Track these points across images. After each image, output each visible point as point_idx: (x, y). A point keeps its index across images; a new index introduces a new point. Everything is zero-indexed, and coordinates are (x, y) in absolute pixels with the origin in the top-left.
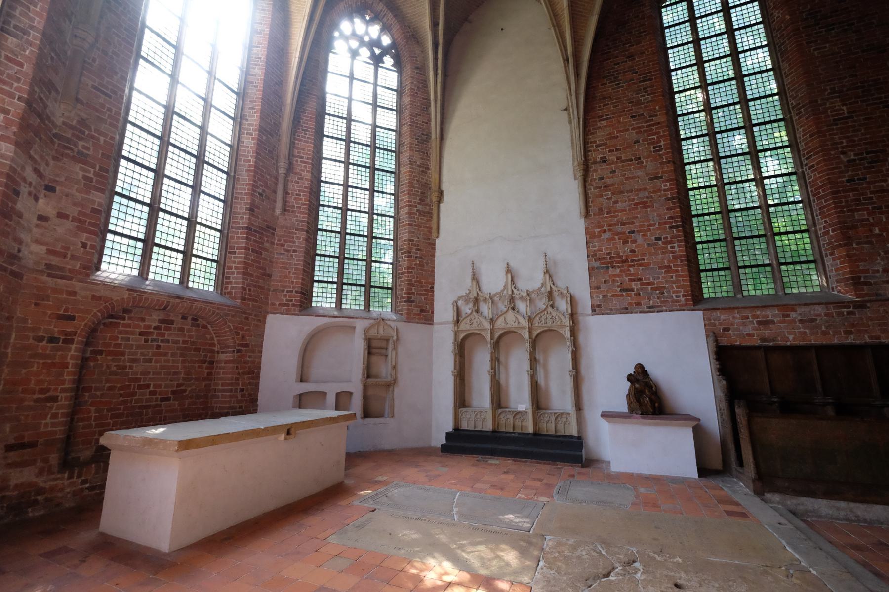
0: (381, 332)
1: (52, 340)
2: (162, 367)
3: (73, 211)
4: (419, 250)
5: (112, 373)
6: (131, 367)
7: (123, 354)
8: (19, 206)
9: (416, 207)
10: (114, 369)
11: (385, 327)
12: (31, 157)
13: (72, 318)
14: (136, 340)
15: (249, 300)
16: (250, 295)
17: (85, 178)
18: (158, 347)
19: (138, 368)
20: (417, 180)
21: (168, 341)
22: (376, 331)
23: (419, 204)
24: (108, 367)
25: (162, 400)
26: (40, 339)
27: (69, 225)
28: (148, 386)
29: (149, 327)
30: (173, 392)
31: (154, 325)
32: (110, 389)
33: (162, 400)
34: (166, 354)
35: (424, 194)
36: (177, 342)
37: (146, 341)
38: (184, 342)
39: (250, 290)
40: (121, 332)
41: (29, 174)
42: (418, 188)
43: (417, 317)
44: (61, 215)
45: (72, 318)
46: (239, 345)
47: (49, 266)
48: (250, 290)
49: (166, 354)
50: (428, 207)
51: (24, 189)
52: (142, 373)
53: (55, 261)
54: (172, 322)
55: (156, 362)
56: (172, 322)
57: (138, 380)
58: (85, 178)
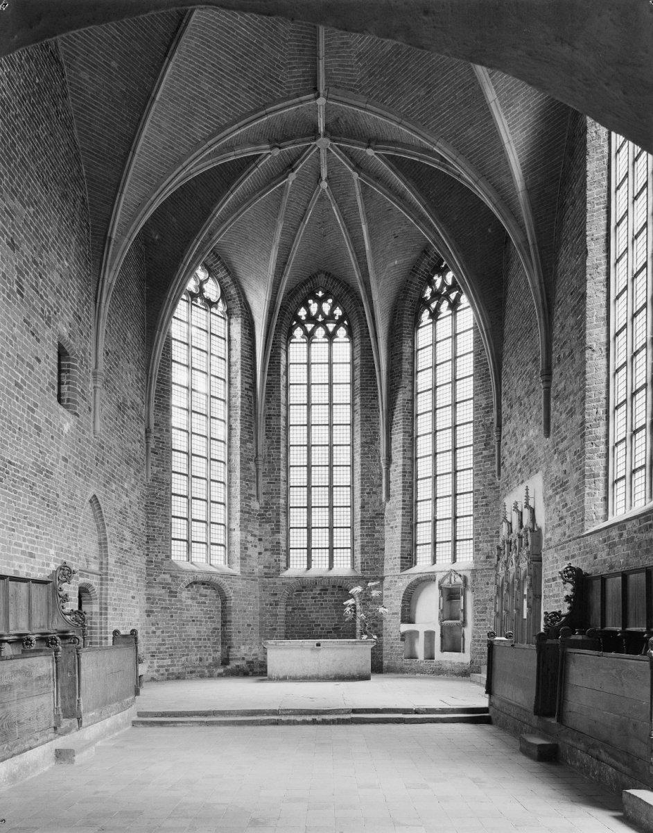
1: (271, 605)
2: (325, 615)
3: (269, 546)
4: (485, 497)
5: (302, 618)
6: (310, 616)
7: (305, 609)
8: (248, 553)
9: (482, 453)
10: (302, 616)
12: (249, 531)
13: (276, 594)
14: (311, 601)
15: (368, 570)
16: (367, 566)
17: (272, 529)
18: (322, 604)
19: (314, 616)
20: (483, 425)
21: (326, 601)
23: (484, 449)
24: (300, 616)
25: (328, 632)
26: (267, 605)
27: (269, 553)
28: (319, 625)
29: (315, 594)
30: (333, 629)
31: (318, 592)
32: (302, 626)
33: (328, 632)
34: (326, 608)
35: (490, 436)
36: (331, 601)
37: (315, 602)
38: (336, 601)
39: (367, 563)
40: (303, 598)
41: (250, 538)
42: (483, 433)
44: (266, 550)
45: (276, 594)
46: (364, 600)
47: (265, 574)
48: (367, 563)
49: (326, 608)
50: (492, 450)
51: (249, 546)
52: (316, 619)
53: (266, 570)
54: (327, 590)
55: (321, 612)
56: (327, 590)
57: (314, 622)
58: (272, 529)
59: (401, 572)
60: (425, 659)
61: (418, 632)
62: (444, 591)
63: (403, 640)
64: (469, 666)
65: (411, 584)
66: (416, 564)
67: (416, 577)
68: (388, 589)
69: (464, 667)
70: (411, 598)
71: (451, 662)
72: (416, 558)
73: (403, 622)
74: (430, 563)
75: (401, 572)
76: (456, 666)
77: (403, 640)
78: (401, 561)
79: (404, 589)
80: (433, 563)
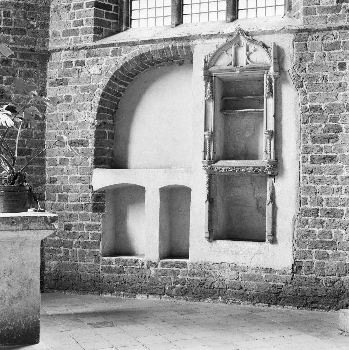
0: (243, 61)
11: (251, 49)
16: (6, 22)
22: (232, 58)
43: (330, 16)
59: (95, 39)
60: (162, 257)
61: (142, 190)
62: (217, 82)
63: (98, 208)
64: (288, 276)
65: (122, 69)
66: (128, 24)
67: (137, 51)
68: (63, 82)
69: (275, 279)
70: (116, 107)
71: (235, 267)
72: (129, 11)
73: (99, 163)
74: (169, 21)
75: (95, 39)
76: (249, 278)
77: (98, 208)
78: (96, 14)
79: (103, 81)
80: (175, 21)
